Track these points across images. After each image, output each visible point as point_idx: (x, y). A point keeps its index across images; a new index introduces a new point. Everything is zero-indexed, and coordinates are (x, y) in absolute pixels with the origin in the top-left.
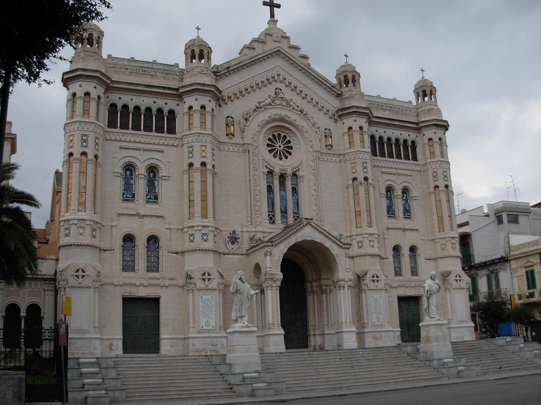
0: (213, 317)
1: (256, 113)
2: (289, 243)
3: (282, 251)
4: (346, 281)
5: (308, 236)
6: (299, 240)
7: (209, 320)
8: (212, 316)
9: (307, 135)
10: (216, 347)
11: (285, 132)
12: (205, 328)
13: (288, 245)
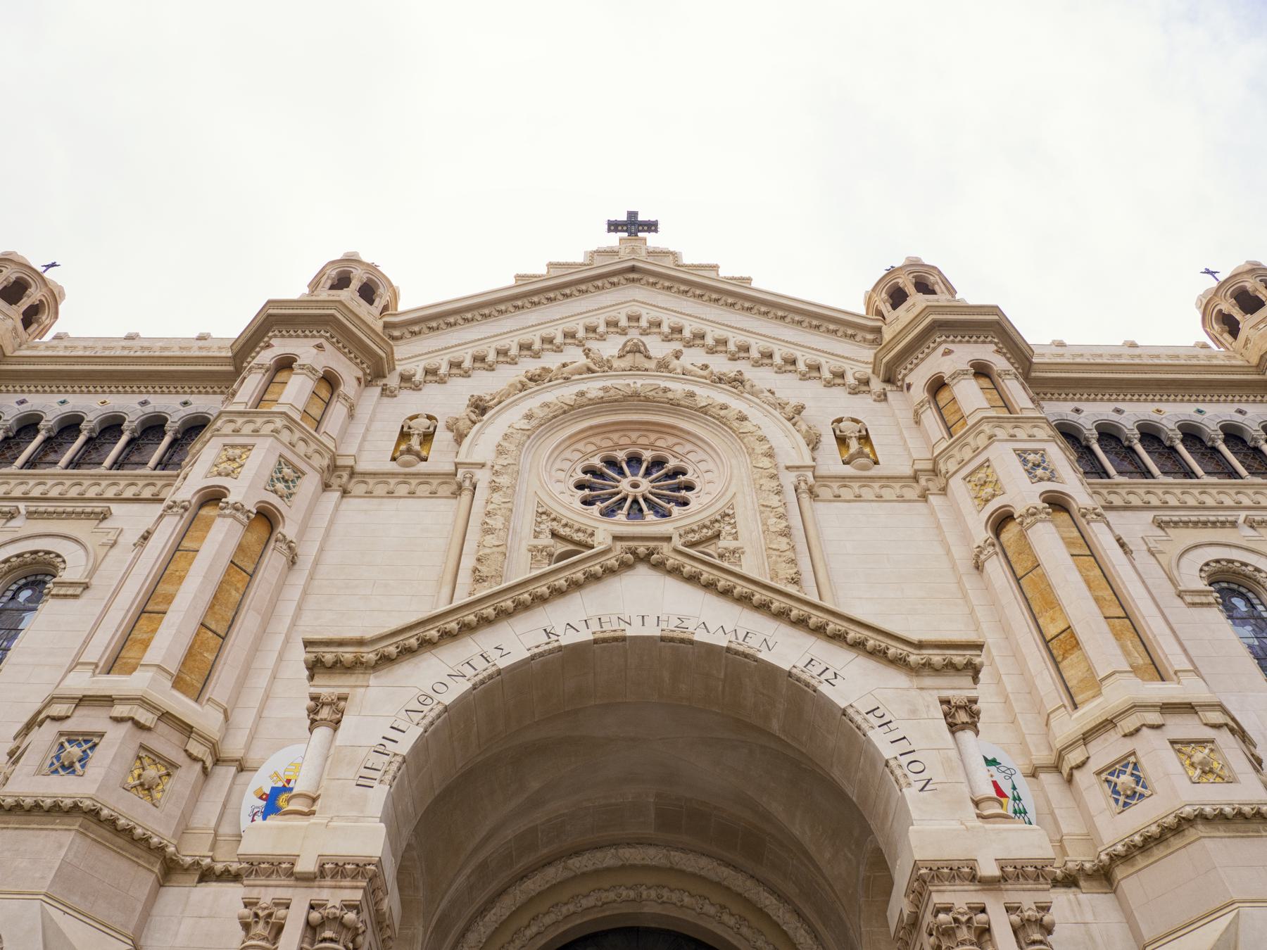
1: (524, 393)
4: (989, 884)
6: (568, 639)
9: (747, 426)
11: (659, 443)
13: (480, 664)
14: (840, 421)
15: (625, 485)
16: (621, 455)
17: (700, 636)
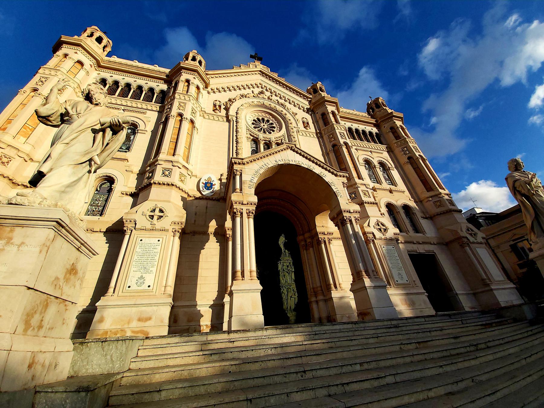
0: (154, 270)
2: (267, 164)
3: (257, 172)
5: (291, 161)
7: (144, 275)
8: (151, 269)
10: (148, 323)
12: (134, 287)
14: (303, 118)
15: (262, 124)
16: (266, 119)
17: (302, 165)
